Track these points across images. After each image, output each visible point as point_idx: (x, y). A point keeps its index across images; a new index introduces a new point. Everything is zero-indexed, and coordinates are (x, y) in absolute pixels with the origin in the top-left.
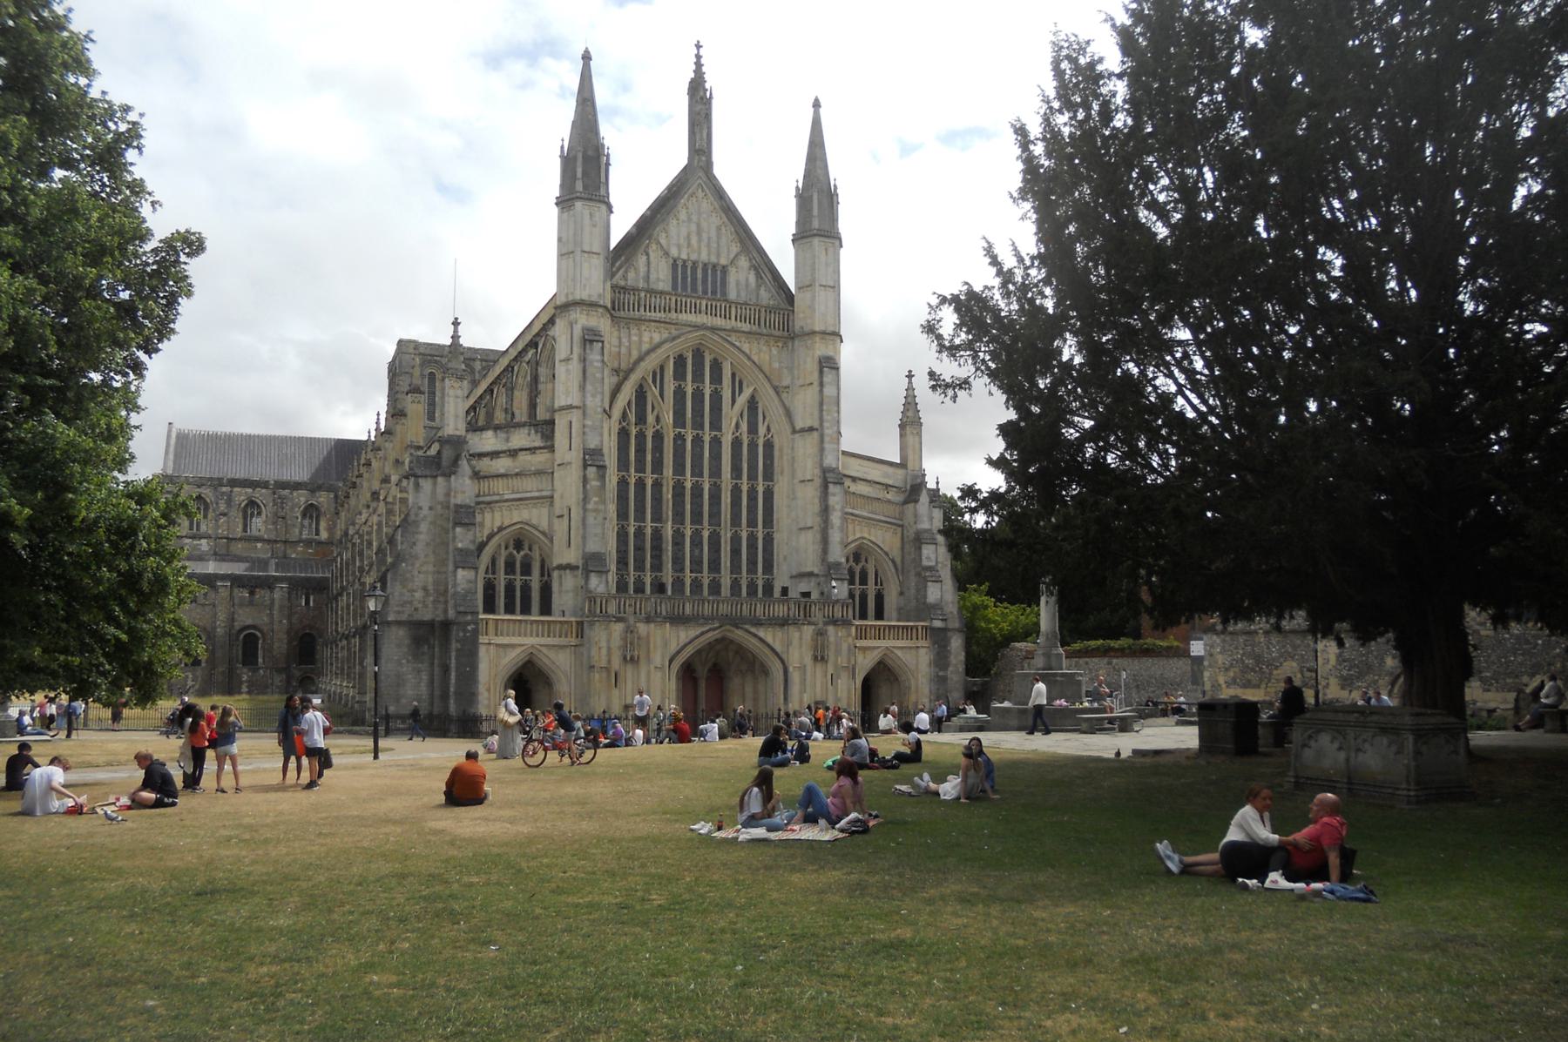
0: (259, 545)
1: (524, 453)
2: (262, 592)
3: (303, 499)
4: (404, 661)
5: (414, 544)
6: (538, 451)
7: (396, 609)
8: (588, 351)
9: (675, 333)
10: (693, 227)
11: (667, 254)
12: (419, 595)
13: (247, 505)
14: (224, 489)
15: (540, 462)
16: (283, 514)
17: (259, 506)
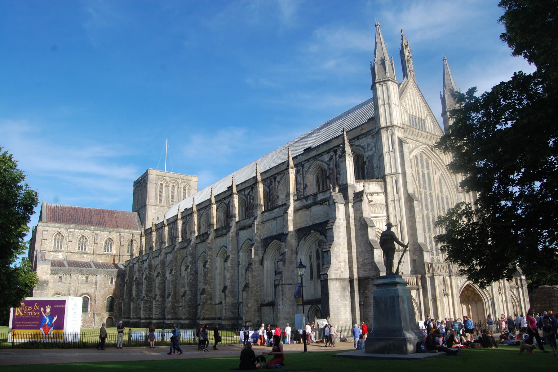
0: (85, 256)
1: (375, 194)
2: (92, 277)
3: (106, 236)
4: (340, 300)
5: (339, 237)
6: (380, 194)
7: (335, 272)
8: (404, 147)
10: (413, 103)
11: (407, 112)
12: (343, 264)
13: (80, 238)
14: (71, 230)
15: (381, 199)
16: (97, 242)
17: (86, 238)
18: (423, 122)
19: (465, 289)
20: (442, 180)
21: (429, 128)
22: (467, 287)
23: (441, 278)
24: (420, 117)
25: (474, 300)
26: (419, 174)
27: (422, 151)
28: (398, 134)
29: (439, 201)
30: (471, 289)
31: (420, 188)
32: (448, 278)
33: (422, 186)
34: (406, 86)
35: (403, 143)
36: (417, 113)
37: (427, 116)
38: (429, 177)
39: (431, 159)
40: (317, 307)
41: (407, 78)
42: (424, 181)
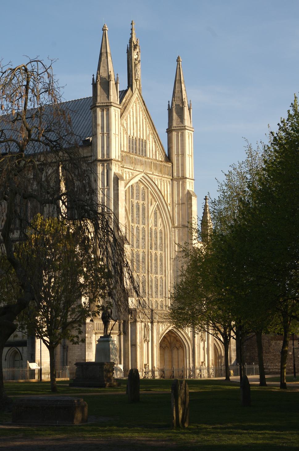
9: (135, 175)
11: (127, 133)
18: (144, 143)
19: (167, 335)
20: (158, 212)
21: (149, 149)
22: (170, 333)
23: (143, 324)
24: (142, 137)
25: (176, 346)
26: (133, 206)
27: (139, 180)
28: (115, 169)
29: (151, 237)
30: (173, 335)
31: (133, 222)
32: (150, 324)
33: (135, 220)
34: (130, 100)
35: (119, 181)
36: (139, 133)
37: (149, 135)
38: (144, 209)
39: (148, 188)
40: (17, 350)
41: (132, 90)
42: (138, 214)
